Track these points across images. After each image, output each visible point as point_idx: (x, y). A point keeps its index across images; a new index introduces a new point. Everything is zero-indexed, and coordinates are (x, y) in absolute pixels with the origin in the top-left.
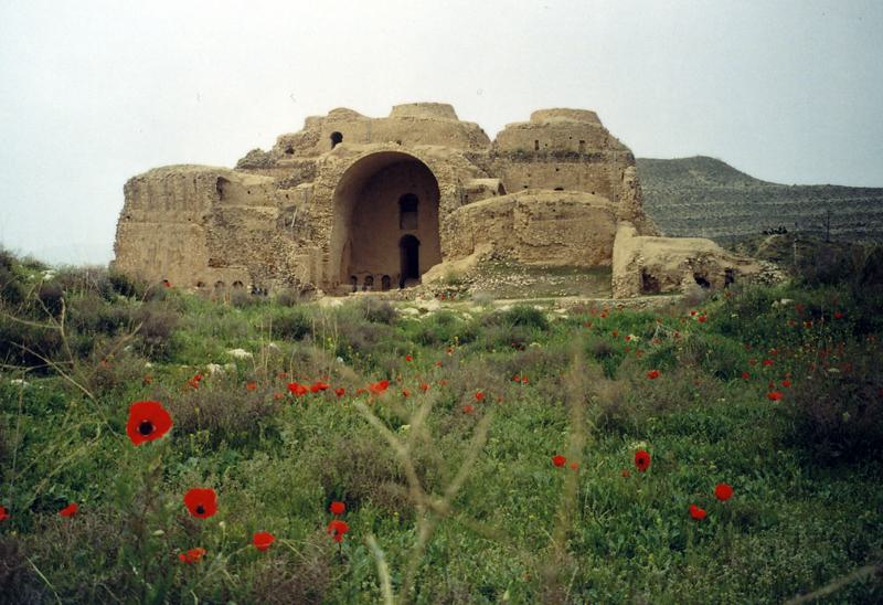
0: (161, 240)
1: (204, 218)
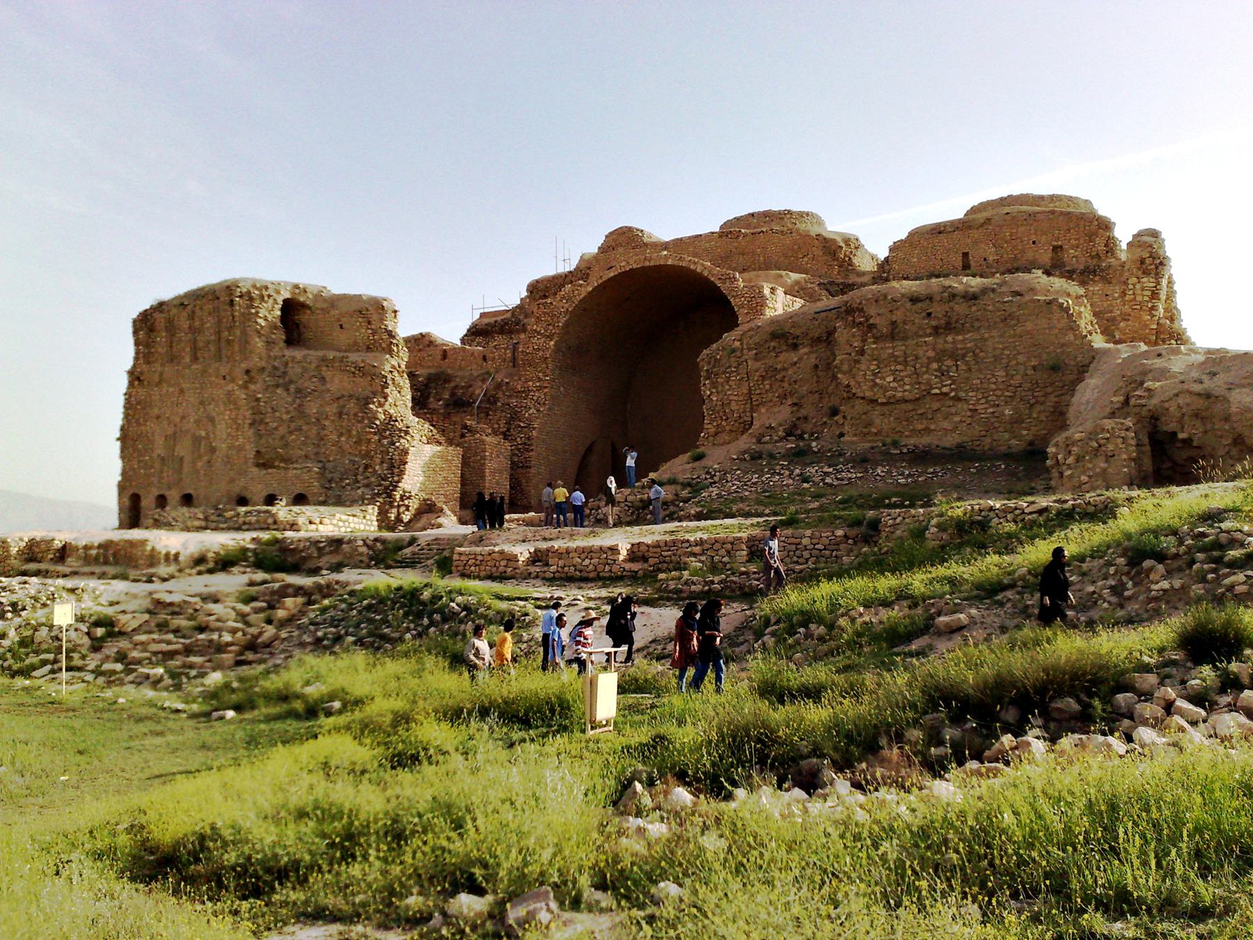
0: (183, 418)
1: (248, 372)
